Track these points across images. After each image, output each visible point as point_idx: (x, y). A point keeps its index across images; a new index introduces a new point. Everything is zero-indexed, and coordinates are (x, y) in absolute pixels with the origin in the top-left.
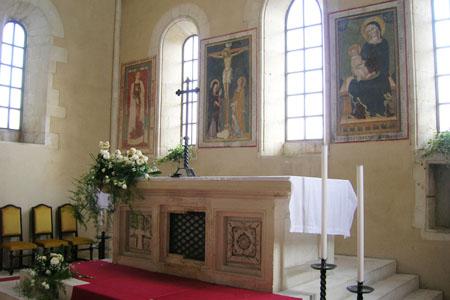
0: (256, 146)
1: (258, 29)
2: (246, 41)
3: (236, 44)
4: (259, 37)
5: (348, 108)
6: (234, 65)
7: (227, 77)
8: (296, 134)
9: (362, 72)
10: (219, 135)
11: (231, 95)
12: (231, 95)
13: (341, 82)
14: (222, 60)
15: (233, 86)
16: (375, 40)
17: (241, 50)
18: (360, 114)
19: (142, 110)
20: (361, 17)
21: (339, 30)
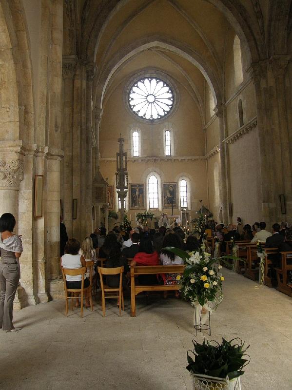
0: (146, 209)
1: (145, 183)
2: (143, 186)
3: (139, 186)
4: (146, 185)
5: (166, 202)
6: (140, 189)
7: (137, 193)
8: (151, 206)
9: (169, 195)
10: (136, 207)
11: (139, 198)
12: (139, 198)
13: (165, 198)
14: (135, 189)
15: (139, 195)
16: (172, 190)
17: (141, 188)
18: (168, 204)
19: (110, 199)
20: (169, 185)
21: (164, 187)
